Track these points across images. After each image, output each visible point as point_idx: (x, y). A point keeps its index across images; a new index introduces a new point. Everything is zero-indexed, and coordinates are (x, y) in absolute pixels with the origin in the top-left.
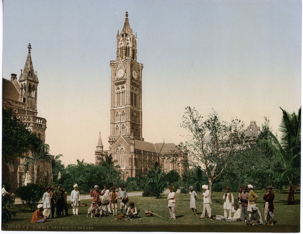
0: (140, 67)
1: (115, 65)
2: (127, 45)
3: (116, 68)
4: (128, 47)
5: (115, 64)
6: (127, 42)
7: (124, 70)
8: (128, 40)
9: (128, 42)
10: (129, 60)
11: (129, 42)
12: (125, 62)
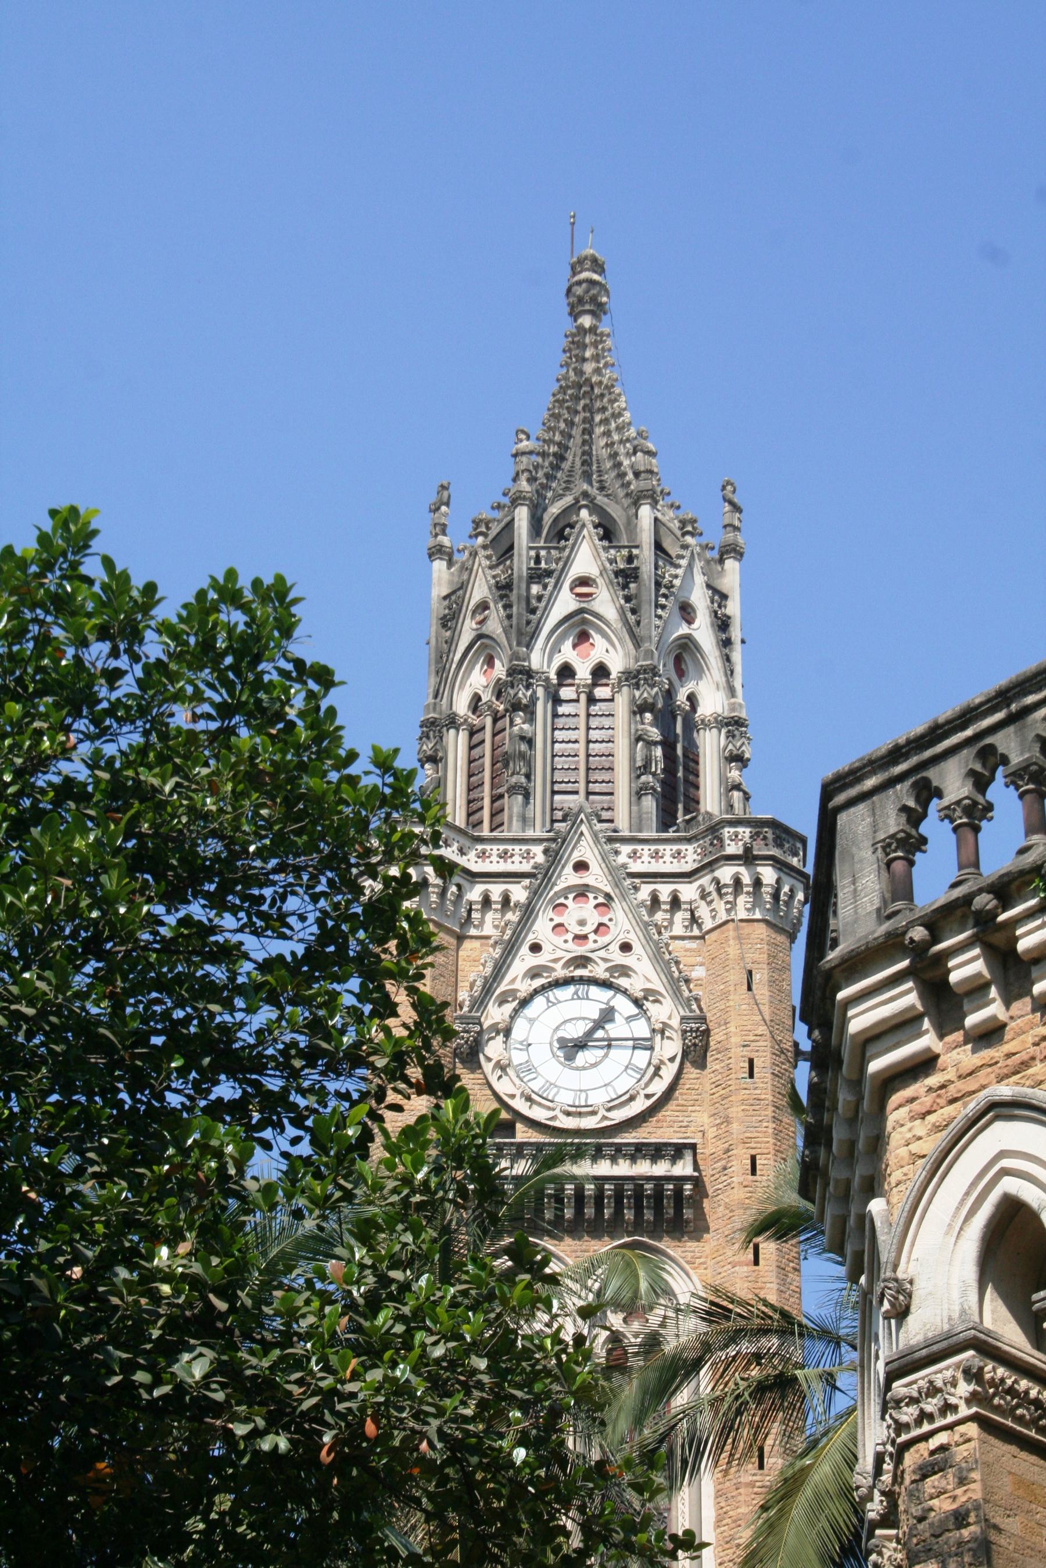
5: (474, 877)
12: (688, 892)
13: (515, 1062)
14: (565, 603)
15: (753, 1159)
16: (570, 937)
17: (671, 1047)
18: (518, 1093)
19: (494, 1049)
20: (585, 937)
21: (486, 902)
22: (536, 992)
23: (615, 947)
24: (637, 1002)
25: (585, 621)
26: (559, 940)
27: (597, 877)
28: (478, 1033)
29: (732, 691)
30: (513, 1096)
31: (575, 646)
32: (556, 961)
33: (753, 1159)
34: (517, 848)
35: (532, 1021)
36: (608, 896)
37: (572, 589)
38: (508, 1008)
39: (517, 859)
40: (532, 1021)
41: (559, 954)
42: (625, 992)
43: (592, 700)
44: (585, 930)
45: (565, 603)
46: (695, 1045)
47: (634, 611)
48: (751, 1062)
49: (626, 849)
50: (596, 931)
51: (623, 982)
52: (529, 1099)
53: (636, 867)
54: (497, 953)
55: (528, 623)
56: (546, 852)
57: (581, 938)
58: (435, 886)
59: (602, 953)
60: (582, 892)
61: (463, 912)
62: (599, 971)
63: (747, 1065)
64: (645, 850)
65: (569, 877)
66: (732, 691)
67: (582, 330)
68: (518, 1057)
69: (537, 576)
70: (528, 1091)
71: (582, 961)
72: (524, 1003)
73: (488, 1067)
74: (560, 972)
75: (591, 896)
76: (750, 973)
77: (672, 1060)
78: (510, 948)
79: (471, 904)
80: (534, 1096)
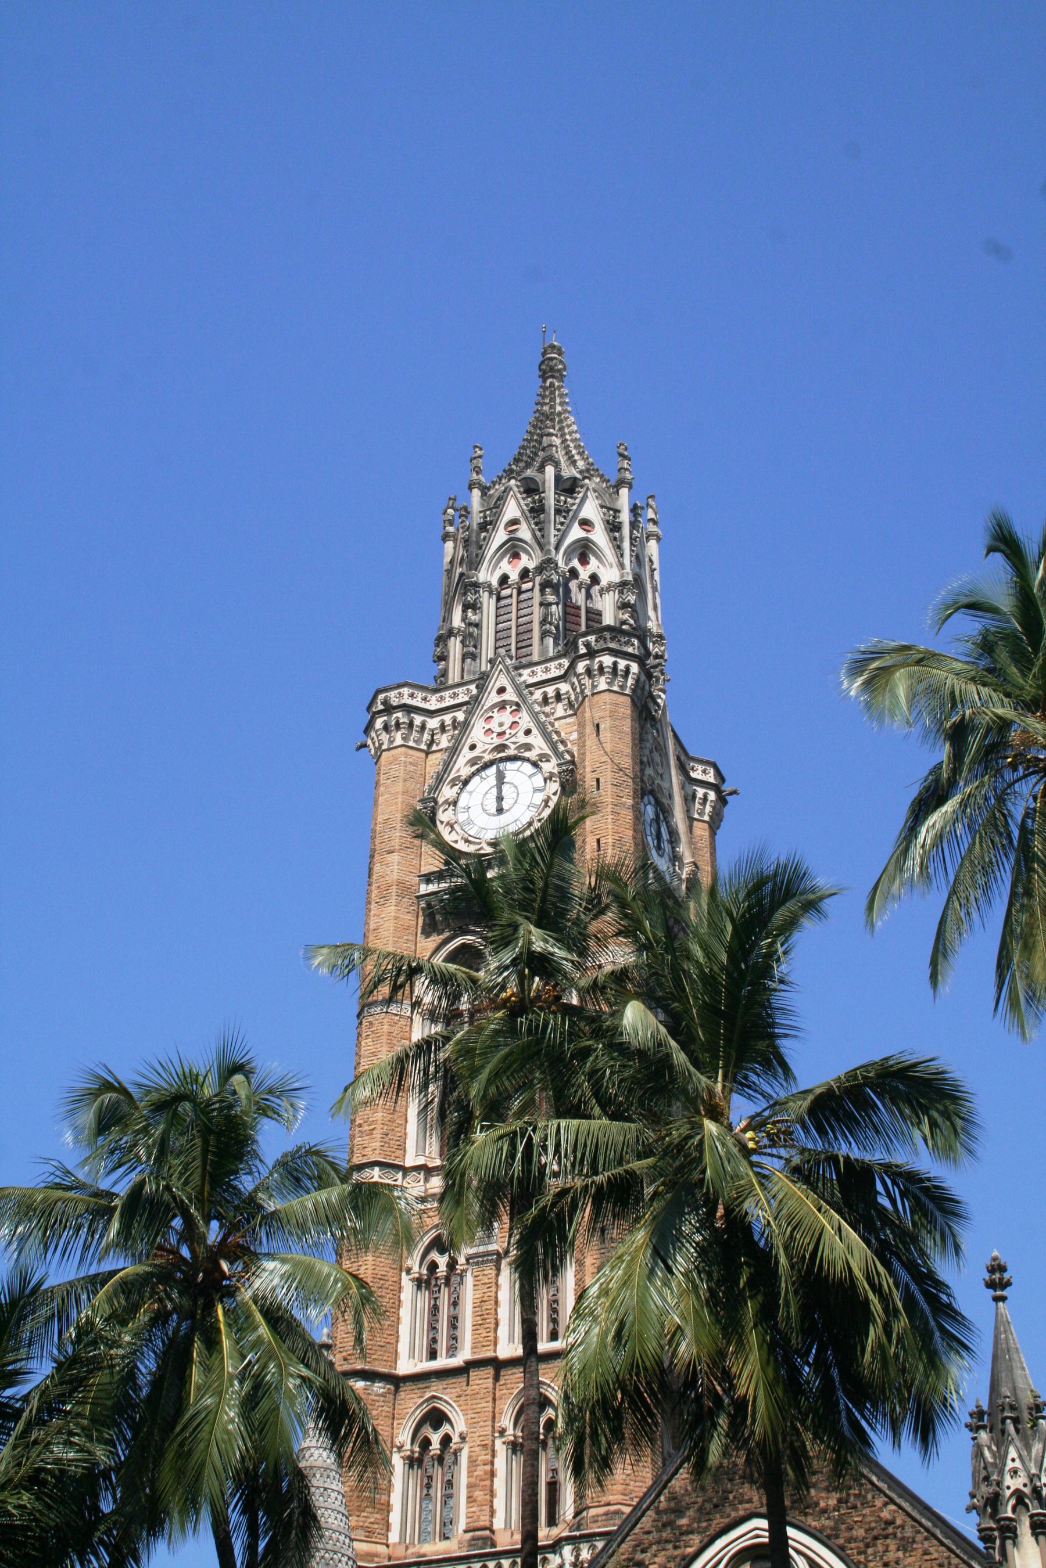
0: (700, 792)
1: (433, 723)
2: (575, 563)
3: (435, 761)
4: (584, 574)
5: (431, 713)
6: (576, 533)
7: (550, 766)
8: (585, 523)
9: (591, 536)
10: (622, 664)
11: (599, 536)
12: (564, 687)
13: (460, 821)
14: (500, 536)
15: (598, 841)
16: (495, 735)
17: (555, 786)
18: (459, 838)
19: (444, 816)
20: (504, 733)
21: (443, 728)
22: (474, 774)
23: (521, 734)
24: (535, 764)
25: (514, 546)
26: (488, 739)
27: (510, 695)
28: (433, 807)
29: (622, 566)
30: (456, 842)
31: (510, 563)
32: (484, 752)
33: (598, 841)
34: (460, 689)
35: (471, 793)
36: (517, 705)
37: (505, 529)
38: (456, 789)
39: (461, 695)
40: (471, 793)
41: (487, 746)
42: (528, 760)
43: (520, 592)
44: (503, 728)
45: (500, 536)
46: (567, 780)
47: (540, 530)
48: (598, 780)
49: (526, 672)
50: (510, 728)
51: (527, 754)
52: (467, 841)
53: (531, 680)
54: (445, 756)
55: (477, 555)
56: (477, 687)
57: (501, 734)
58: (404, 723)
59: (513, 740)
60: (502, 706)
61: (426, 737)
62: (511, 752)
63: (595, 783)
64: (538, 669)
65: (493, 698)
66: (622, 566)
67: (545, 388)
68: (462, 817)
69: (483, 527)
70: (466, 836)
71: (502, 748)
72: (466, 783)
73: (440, 827)
74: (487, 757)
75: (508, 707)
76: (598, 725)
77: (555, 794)
78: (453, 751)
79: (433, 730)
80: (470, 838)
